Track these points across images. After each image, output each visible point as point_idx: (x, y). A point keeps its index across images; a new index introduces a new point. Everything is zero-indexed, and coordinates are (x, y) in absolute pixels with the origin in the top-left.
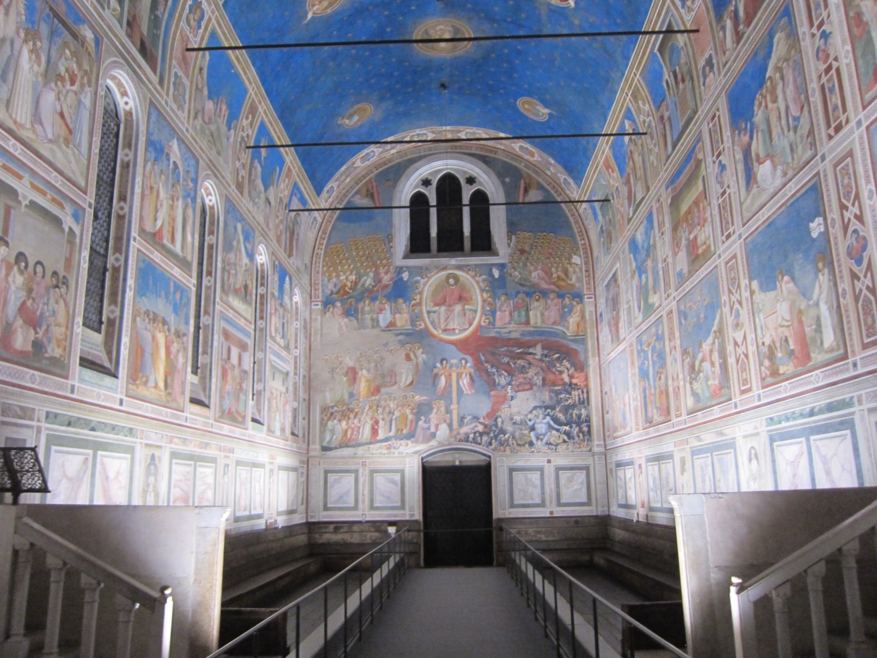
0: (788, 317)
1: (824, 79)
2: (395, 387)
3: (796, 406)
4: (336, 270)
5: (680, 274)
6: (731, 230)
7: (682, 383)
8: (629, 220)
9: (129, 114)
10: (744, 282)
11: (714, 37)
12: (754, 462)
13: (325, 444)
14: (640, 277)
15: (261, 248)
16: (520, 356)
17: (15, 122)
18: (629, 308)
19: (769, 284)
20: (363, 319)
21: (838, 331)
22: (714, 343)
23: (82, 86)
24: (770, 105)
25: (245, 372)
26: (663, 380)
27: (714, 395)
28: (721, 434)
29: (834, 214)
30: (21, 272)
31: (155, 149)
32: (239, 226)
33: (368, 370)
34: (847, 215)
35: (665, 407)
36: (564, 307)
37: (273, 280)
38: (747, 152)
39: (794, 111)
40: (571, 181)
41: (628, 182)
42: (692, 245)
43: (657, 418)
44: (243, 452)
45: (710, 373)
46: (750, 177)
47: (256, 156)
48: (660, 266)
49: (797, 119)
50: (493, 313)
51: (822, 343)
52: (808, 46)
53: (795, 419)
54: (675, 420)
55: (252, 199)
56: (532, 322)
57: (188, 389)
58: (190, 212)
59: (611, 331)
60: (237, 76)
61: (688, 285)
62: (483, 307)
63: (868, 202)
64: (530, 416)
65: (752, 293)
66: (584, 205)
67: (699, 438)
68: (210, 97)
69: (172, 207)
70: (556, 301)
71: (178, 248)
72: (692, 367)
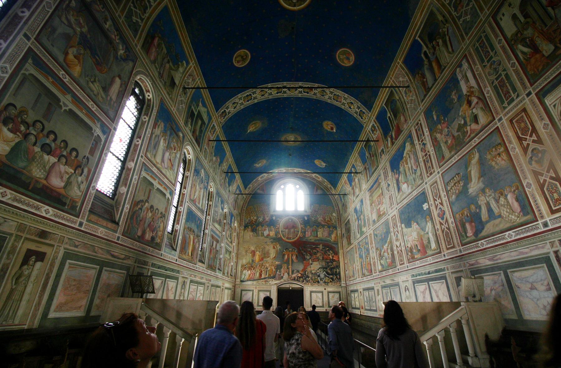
0: (416, 237)
1: (425, 158)
2: (269, 258)
3: (422, 270)
4: (250, 215)
5: (374, 221)
6: (393, 206)
7: (376, 261)
8: (354, 201)
9: (190, 160)
10: (399, 224)
11: (384, 143)
12: (407, 291)
13: (242, 279)
14: (358, 221)
15: (226, 206)
16: (315, 248)
17: (156, 162)
18: (354, 232)
19: (408, 225)
20: (258, 233)
21: (437, 243)
22: (388, 246)
23: (177, 151)
24: (405, 165)
25: (217, 251)
26: (369, 259)
27: (389, 266)
28: (393, 280)
29: (432, 202)
30: (151, 212)
31: (197, 172)
32: (220, 199)
33: (259, 252)
34: (436, 203)
35: (370, 268)
36: (330, 231)
37: (229, 218)
38: (398, 181)
39: (414, 168)
40: (332, 187)
41: (353, 189)
42: (379, 211)
43: (367, 273)
44: (214, 282)
45: (387, 257)
46: (399, 189)
47: (227, 175)
48: (366, 218)
49: (416, 170)
50: (305, 233)
51: (431, 247)
52: (418, 147)
53: (422, 275)
54: (374, 274)
55: (224, 190)
56: (319, 236)
57: (199, 256)
58: (205, 193)
59: (347, 240)
60: (224, 149)
61: (377, 225)
62: (301, 230)
64: (318, 271)
65: (402, 229)
66: (337, 196)
67: (384, 282)
68: (215, 156)
69: (200, 192)
70: (327, 229)
71: (200, 206)
72: (380, 254)
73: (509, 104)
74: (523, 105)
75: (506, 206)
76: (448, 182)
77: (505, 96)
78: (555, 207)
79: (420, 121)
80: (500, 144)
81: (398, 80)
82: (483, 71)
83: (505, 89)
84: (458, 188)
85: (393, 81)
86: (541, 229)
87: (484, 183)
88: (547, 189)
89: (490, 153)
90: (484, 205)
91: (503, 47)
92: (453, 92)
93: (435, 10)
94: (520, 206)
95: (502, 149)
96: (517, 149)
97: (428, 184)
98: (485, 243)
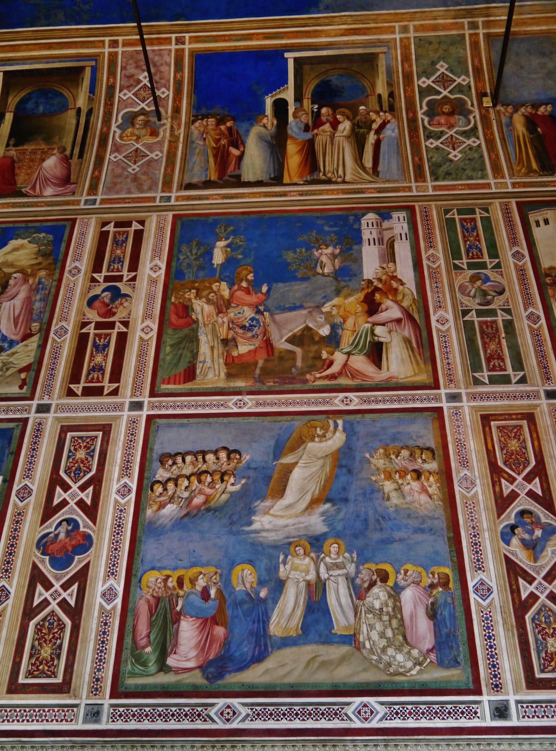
63: (114, 496)
73: (493, 381)
74: (529, 406)
75: (386, 618)
76: (173, 456)
77: (488, 360)
78: (542, 671)
79: (142, 223)
80: (431, 450)
81: (131, 70)
82: (448, 272)
83: (493, 346)
84: (208, 491)
85: (113, 57)
86: (484, 719)
87: (328, 519)
88: (533, 620)
89: (387, 456)
90: (302, 585)
91: (521, 272)
92: (327, 246)
93: (382, 63)
94: (437, 632)
95: (433, 466)
96: (478, 489)
97: (51, 416)
98: (244, 711)
